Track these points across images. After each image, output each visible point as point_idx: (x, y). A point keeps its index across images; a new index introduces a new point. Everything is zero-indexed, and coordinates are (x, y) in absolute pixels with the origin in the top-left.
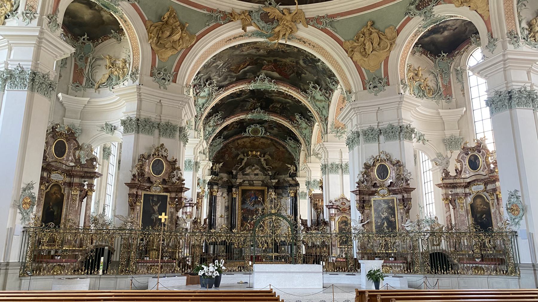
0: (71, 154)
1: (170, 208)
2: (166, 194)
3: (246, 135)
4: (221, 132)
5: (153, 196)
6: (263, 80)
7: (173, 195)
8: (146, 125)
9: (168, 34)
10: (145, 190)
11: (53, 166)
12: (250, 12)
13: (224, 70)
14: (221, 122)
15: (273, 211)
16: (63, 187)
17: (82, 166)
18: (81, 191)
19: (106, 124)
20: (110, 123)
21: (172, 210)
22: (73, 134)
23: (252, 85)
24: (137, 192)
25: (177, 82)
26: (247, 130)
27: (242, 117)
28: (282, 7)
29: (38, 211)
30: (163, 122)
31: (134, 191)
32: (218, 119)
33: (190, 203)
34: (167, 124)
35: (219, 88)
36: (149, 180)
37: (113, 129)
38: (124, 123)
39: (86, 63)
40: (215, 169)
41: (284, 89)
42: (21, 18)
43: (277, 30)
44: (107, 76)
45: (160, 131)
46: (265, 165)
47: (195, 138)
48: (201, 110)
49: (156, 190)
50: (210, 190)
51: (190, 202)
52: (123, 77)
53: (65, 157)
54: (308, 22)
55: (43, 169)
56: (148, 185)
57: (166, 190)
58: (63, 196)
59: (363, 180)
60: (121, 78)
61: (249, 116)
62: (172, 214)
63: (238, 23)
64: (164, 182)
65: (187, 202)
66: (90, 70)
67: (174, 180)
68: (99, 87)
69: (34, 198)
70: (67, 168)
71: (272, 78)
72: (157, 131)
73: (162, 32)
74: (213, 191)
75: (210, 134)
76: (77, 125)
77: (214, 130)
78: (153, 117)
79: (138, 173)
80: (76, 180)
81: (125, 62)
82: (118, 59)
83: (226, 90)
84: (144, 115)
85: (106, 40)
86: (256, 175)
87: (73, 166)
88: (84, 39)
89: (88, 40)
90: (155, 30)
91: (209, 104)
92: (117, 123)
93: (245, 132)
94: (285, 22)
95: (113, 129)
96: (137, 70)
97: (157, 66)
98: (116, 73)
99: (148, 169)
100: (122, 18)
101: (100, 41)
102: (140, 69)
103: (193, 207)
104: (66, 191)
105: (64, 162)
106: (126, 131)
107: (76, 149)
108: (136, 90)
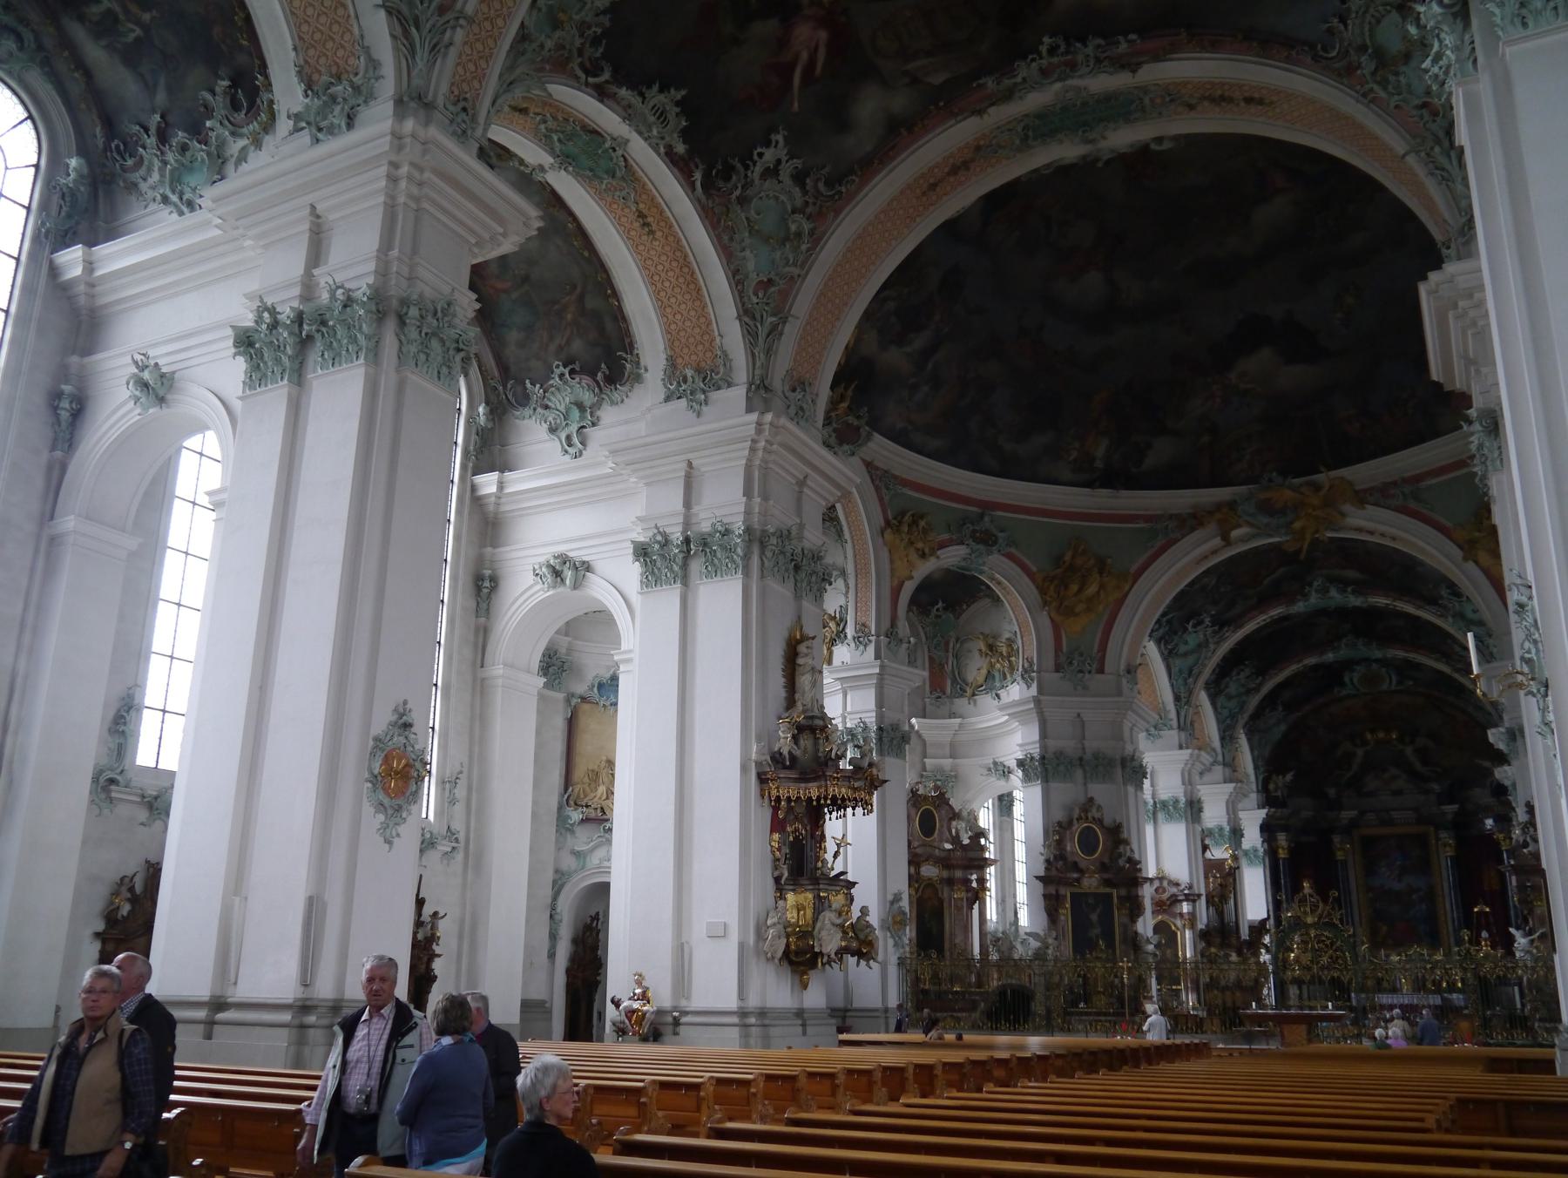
0: (945, 829)
1: (1119, 918)
2: (1108, 890)
3: (1344, 692)
4: (1271, 700)
5: (1086, 895)
6: (1324, 591)
7: (1123, 892)
8: (1058, 765)
9: (1074, 588)
10: (1071, 885)
11: (920, 855)
12: (1232, 505)
13: (1222, 590)
14: (1258, 681)
15: (1309, 920)
16: (938, 886)
17: (964, 848)
18: (967, 891)
19: (995, 763)
20: (1001, 760)
21: (1126, 920)
22: (942, 795)
23: (1301, 604)
24: (1057, 891)
25: (1107, 669)
26: (1347, 679)
27: (1311, 661)
28: (1296, 481)
29: (910, 930)
30: (1088, 756)
31: (1052, 890)
32: (1247, 677)
33: (1185, 895)
34: (1096, 756)
35: (1222, 626)
36: (1075, 867)
37: (1006, 772)
38: (1021, 764)
39: (947, 651)
40: (1276, 791)
41: (1381, 601)
42: (853, 645)
43: (1297, 525)
44: (984, 672)
45: (1085, 771)
46: (1418, 766)
47: (1181, 747)
48: (1186, 684)
49: (1091, 883)
50: (1269, 845)
51: (1186, 892)
52: (1012, 674)
53: (936, 835)
54: (1361, 498)
55: (910, 863)
56: (1075, 875)
57: (1108, 883)
58: (941, 901)
59: (1525, 841)
60: (1008, 676)
61: (1330, 657)
62: (1125, 927)
63: (1212, 527)
64: (1103, 867)
65: (1182, 891)
66: (955, 663)
67: (1121, 862)
68: (974, 695)
69: (904, 913)
70: (943, 854)
71: (1343, 584)
72: (1079, 773)
73: (1066, 587)
74: (1278, 847)
75: (1233, 716)
76: (948, 768)
77: (1242, 706)
78: (1069, 745)
79: (1055, 857)
80: (959, 874)
81: (1010, 642)
82: (1000, 636)
83: (1241, 627)
84: (1053, 744)
85: (974, 602)
86: (1398, 793)
87: (949, 850)
88: (937, 610)
89: (945, 609)
90: (1052, 588)
91: (1205, 666)
92: (1013, 764)
93: (1342, 684)
94: (1310, 511)
95: (1006, 772)
96: (1031, 664)
97: (1065, 649)
98: (998, 665)
99: (1073, 847)
100: (992, 579)
101: (965, 607)
102: (1035, 661)
103: (1194, 901)
104: (945, 893)
105: (936, 844)
106: (1027, 778)
107: (951, 819)
108: (1032, 706)
